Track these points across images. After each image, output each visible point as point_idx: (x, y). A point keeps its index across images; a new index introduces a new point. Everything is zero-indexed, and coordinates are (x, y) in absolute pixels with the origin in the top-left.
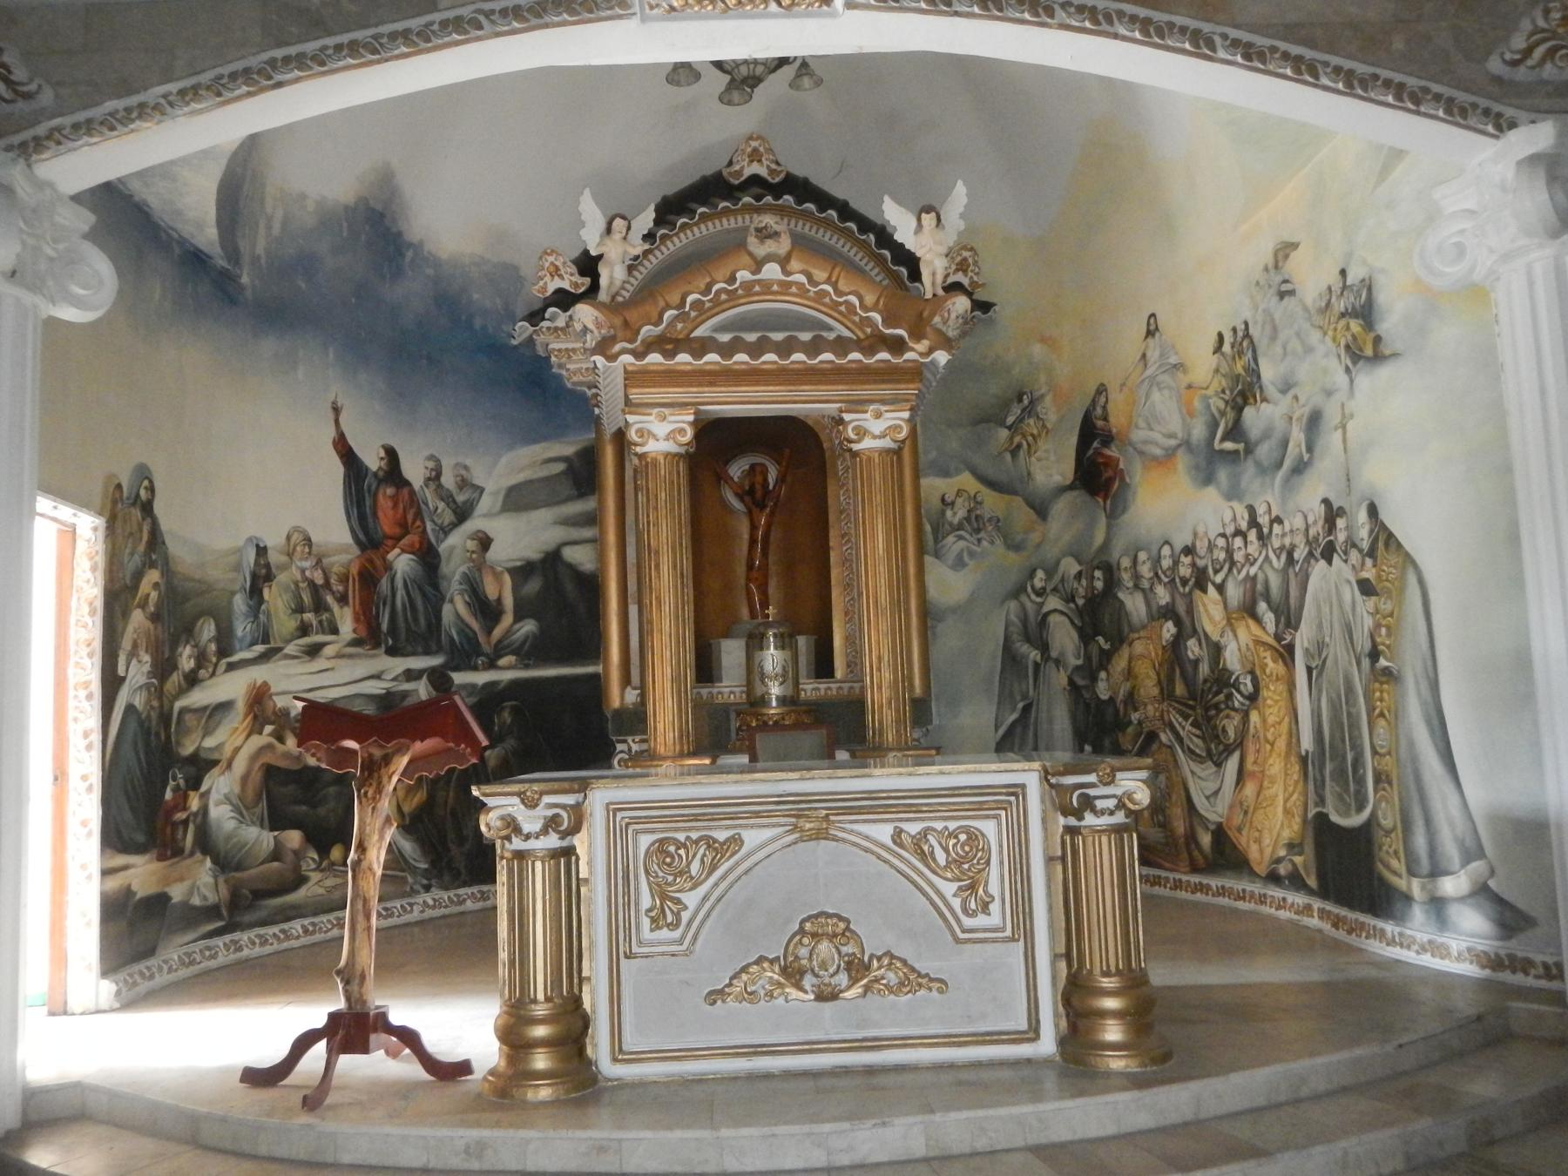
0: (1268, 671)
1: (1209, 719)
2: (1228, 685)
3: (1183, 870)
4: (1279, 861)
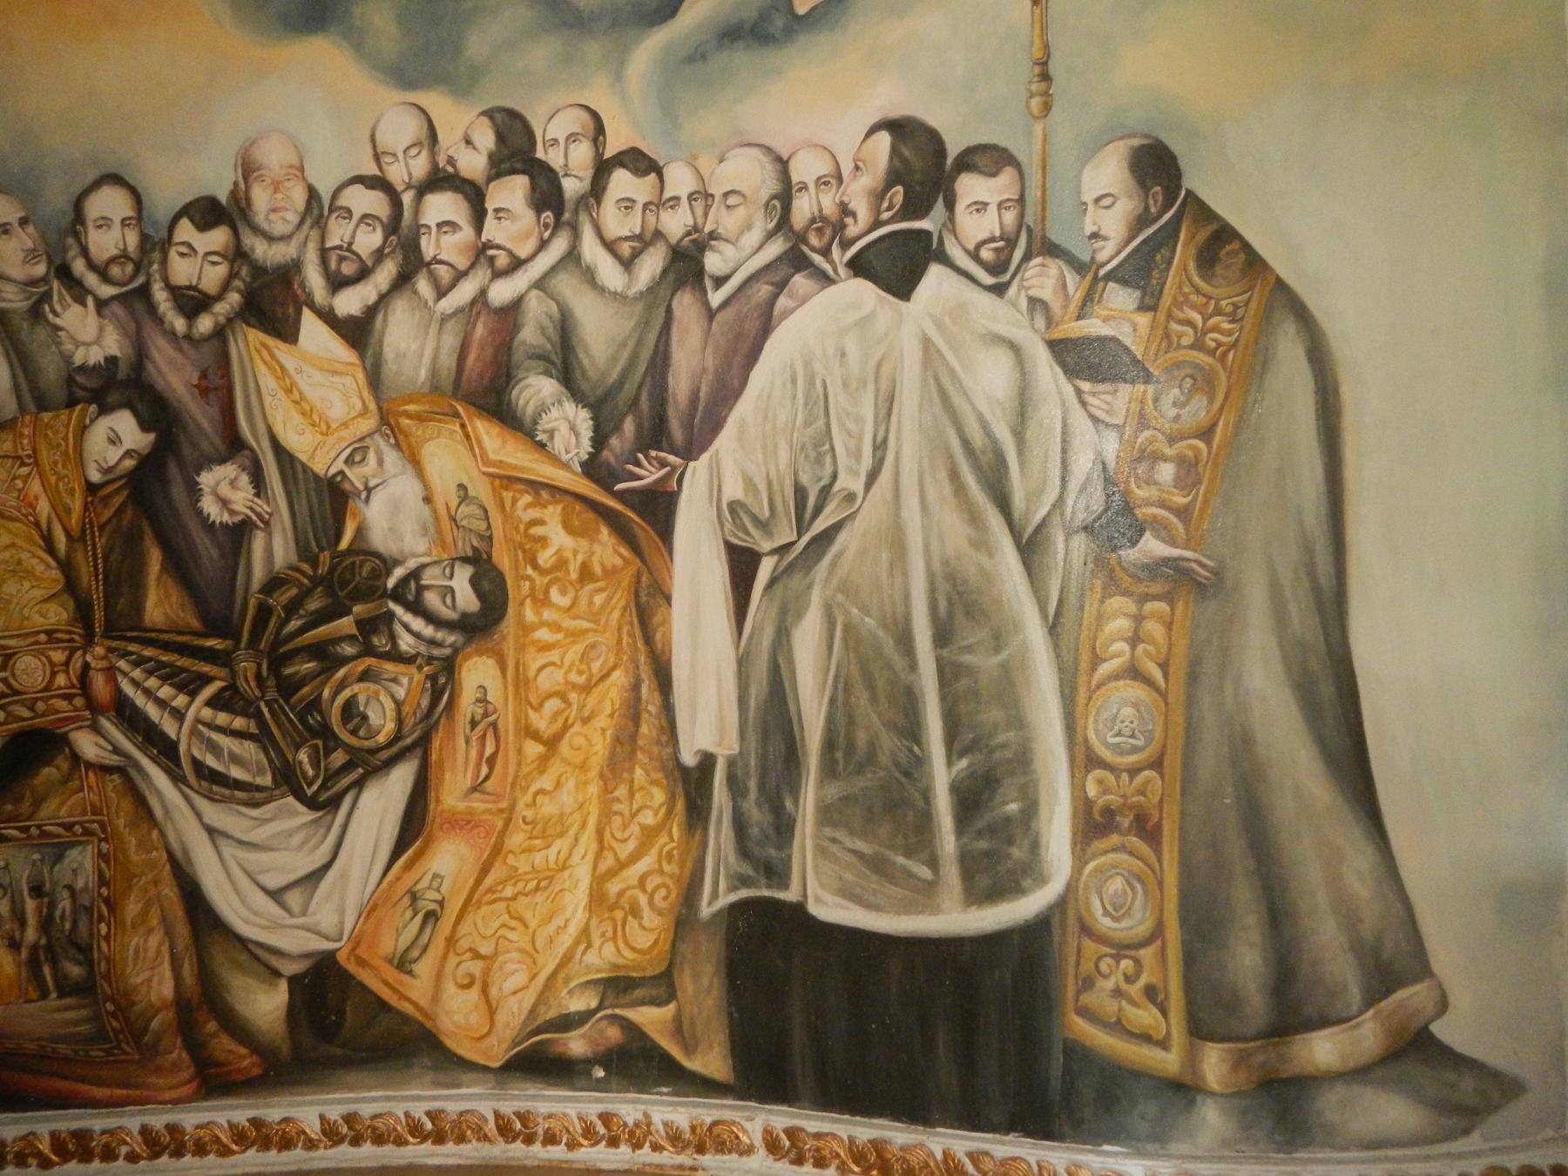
0: (545, 557)
1: (288, 688)
2: (372, 590)
3: (168, 1095)
4: (567, 1023)
